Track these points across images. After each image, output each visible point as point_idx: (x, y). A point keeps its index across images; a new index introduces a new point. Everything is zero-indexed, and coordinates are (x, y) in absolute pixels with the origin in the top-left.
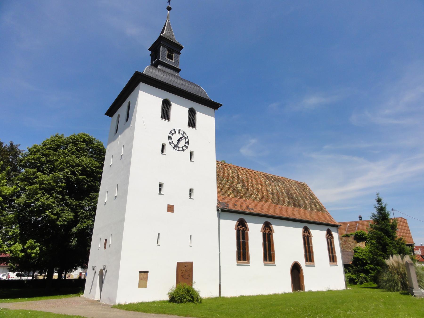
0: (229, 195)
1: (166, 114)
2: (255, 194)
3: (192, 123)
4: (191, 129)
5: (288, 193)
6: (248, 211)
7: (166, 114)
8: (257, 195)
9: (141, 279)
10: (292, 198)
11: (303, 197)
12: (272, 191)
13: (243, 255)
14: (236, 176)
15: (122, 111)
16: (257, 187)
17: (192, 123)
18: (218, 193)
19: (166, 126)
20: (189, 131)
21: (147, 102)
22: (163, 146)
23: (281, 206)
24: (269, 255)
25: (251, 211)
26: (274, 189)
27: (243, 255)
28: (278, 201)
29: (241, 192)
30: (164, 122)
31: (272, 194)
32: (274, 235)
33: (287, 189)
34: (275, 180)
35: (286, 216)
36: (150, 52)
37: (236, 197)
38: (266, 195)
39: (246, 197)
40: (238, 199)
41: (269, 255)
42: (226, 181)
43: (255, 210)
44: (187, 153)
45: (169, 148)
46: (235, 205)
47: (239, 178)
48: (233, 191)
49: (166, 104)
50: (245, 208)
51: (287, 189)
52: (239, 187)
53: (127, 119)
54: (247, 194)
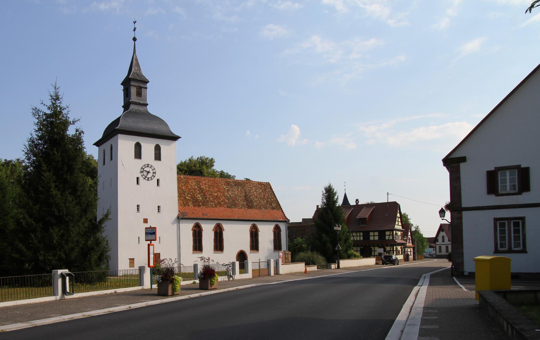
0: (189, 206)
1: (138, 154)
2: (212, 202)
3: (158, 157)
4: (158, 162)
5: (246, 196)
6: (202, 217)
7: (138, 154)
8: (214, 202)
9: (130, 263)
10: (248, 200)
11: (261, 198)
12: (230, 196)
13: (198, 246)
14: (198, 187)
15: (106, 146)
16: (216, 194)
17: (158, 157)
18: (180, 205)
19: (139, 163)
20: (156, 164)
21: (125, 145)
22: (138, 178)
23: (234, 209)
24: (219, 246)
25: (205, 217)
26: (232, 194)
27: (198, 246)
28: (233, 204)
29: (200, 202)
30: (138, 161)
31: (228, 199)
32: (224, 232)
33: (245, 193)
34: (235, 185)
35: (236, 218)
36: (122, 87)
37: (194, 206)
38: (222, 201)
39: (204, 205)
40: (197, 208)
41: (219, 246)
42: (188, 194)
43: (209, 216)
44: (155, 180)
45: (141, 179)
46: (193, 213)
47: (200, 188)
48: (193, 202)
49: (138, 147)
50: (201, 214)
51: (245, 193)
52: (199, 197)
53: (111, 159)
54: (205, 203)
